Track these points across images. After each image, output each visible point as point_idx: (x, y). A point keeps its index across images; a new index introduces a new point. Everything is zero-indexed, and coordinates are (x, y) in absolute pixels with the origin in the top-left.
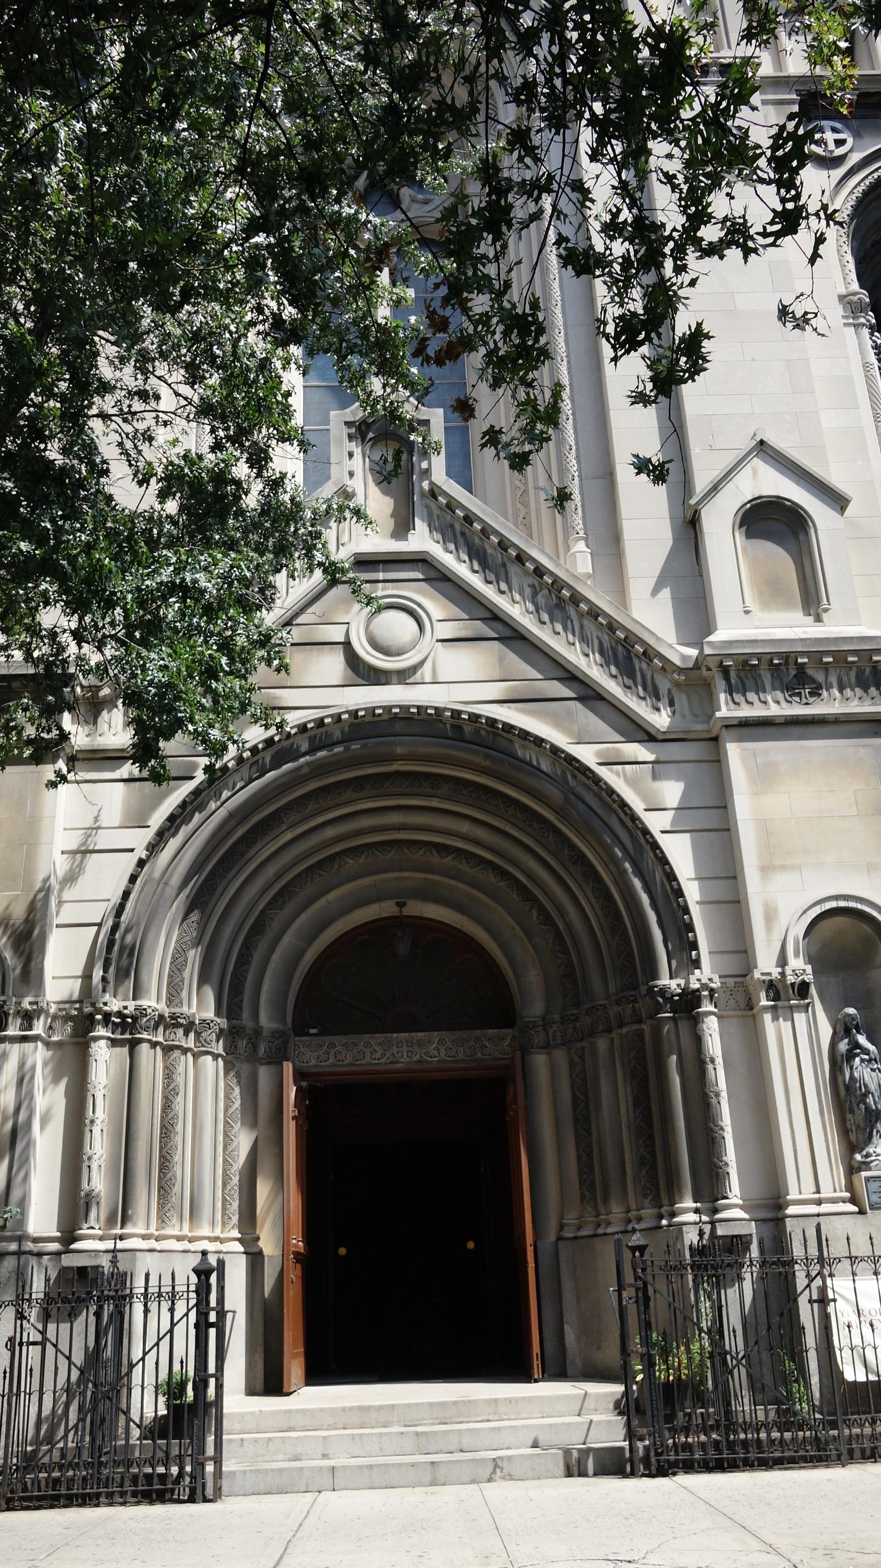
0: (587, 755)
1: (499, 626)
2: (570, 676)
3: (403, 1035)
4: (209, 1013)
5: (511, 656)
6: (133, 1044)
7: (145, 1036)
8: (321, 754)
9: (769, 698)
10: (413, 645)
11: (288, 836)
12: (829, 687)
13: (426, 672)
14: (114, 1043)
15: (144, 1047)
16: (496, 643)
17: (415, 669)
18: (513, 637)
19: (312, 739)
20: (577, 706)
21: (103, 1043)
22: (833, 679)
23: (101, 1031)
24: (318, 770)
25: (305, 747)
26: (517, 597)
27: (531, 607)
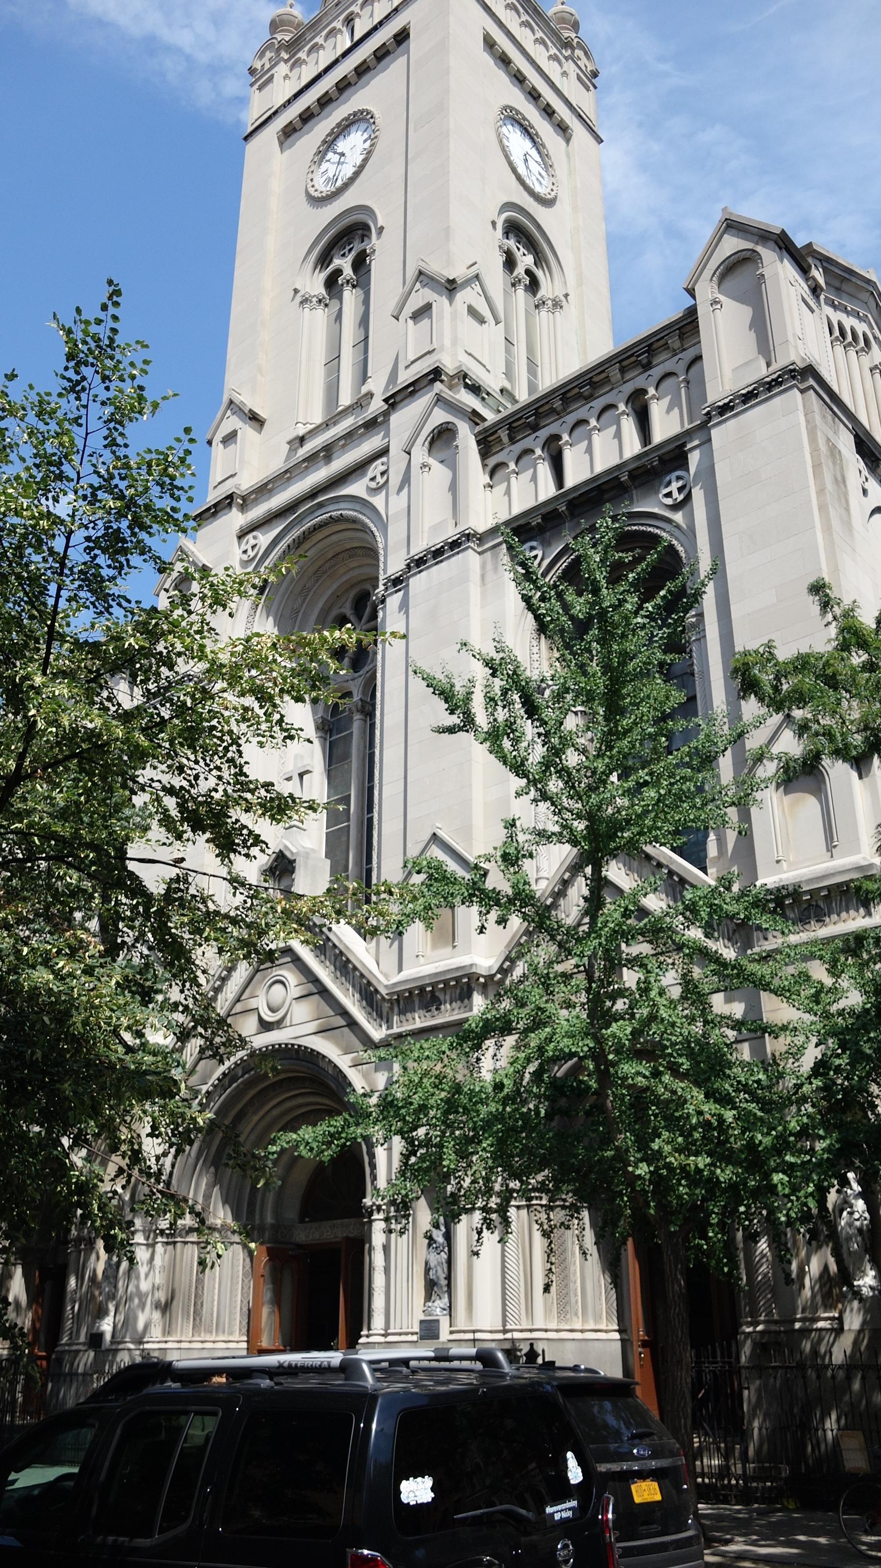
0: (343, 1062)
1: (318, 985)
2: (344, 1013)
3: (339, 1221)
4: (229, 1221)
5: (323, 1003)
6: (175, 1243)
7: (179, 1239)
8: (246, 1076)
9: (417, 1016)
10: (284, 1002)
11: (256, 1118)
12: (445, 1002)
13: (287, 1021)
14: (167, 1243)
15: (179, 1245)
16: (317, 996)
17: (284, 1018)
18: (323, 992)
19: (243, 1068)
20: (346, 1030)
21: (159, 1245)
22: (448, 997)
23: (159, 1239)
24: (249, 1084)
25: (240, 1073)
26: (328, 963)
27: (332, 968)
